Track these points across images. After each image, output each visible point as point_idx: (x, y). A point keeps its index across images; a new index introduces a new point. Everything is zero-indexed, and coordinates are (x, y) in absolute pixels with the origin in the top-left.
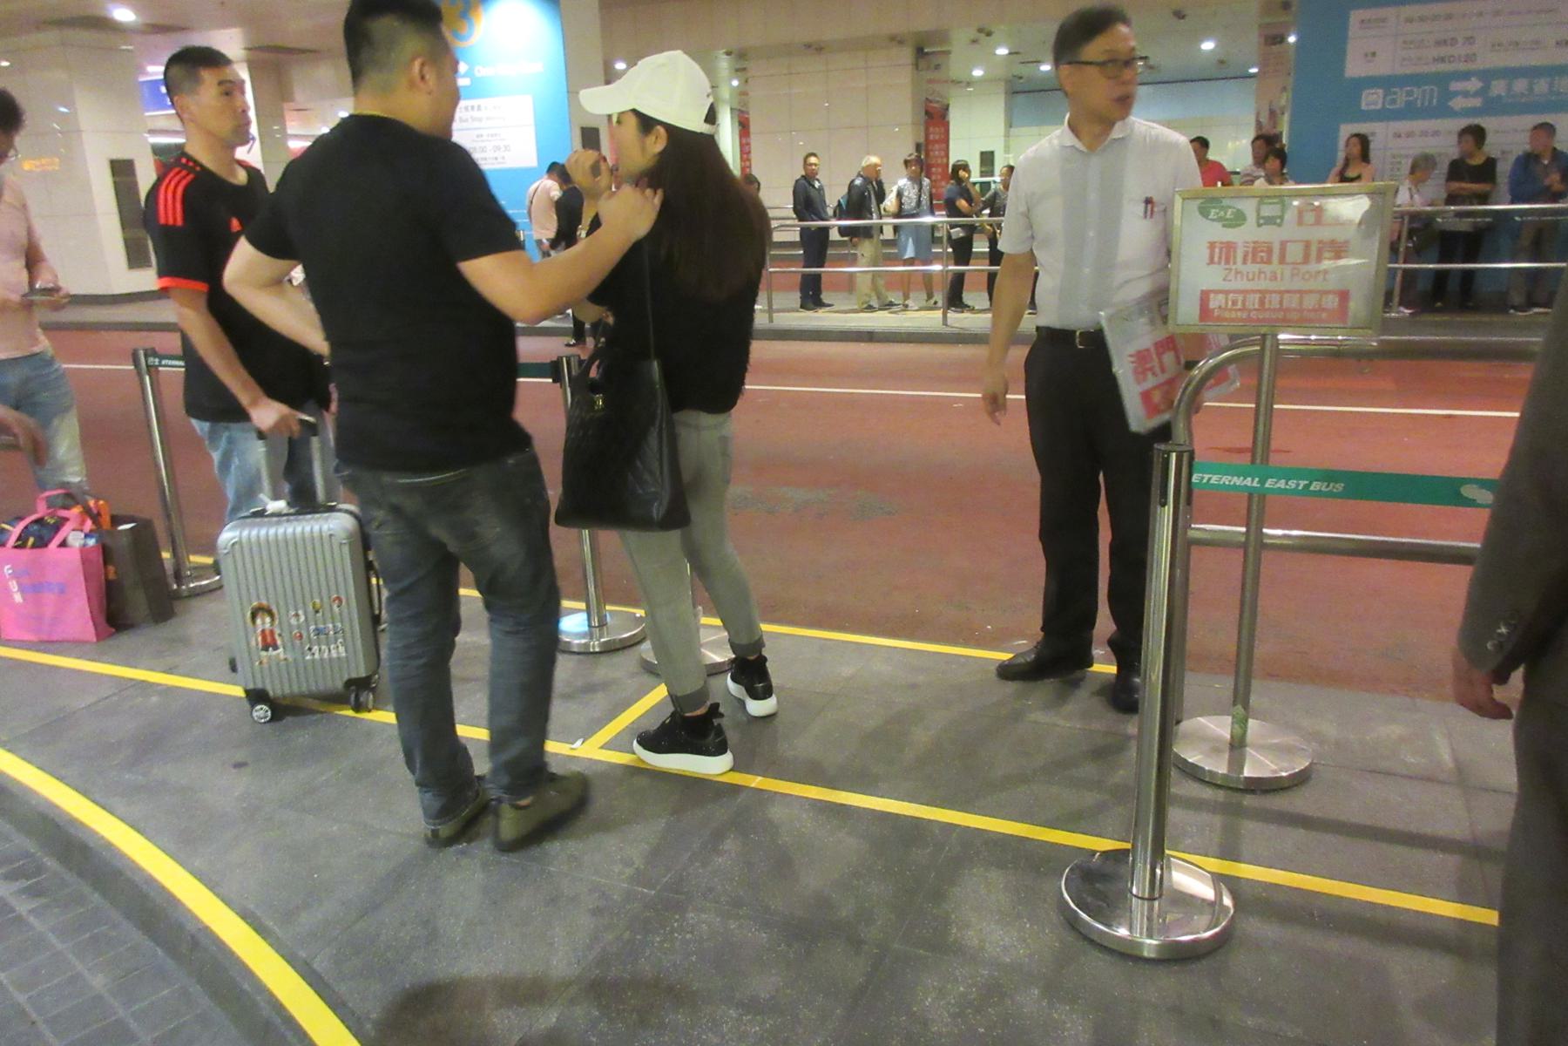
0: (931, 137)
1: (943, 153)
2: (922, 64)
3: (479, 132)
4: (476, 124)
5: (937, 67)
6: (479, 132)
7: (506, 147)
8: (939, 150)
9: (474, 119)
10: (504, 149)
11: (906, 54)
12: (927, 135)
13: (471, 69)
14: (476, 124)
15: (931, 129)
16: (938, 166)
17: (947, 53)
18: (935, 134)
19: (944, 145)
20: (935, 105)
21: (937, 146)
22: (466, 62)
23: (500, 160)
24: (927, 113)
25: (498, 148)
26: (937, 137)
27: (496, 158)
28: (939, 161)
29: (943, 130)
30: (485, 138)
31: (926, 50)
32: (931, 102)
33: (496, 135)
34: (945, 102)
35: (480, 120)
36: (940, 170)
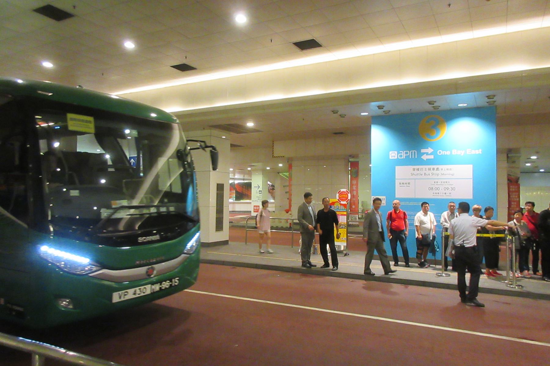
0: (511, 190)
4: (436, 177)
6: (436, 181)
8: (515, 195)
9: (433, 174)
10: (451, 189)
14: (436, 177)
15: (511, 187)
16: (514, 201)
17: (520, 157)
19: (517, 193)
21: (514, 194)
24: (508, 180)
26: (514, 190)
27: (445, 193)
28: (515, 199)
32: (510, 175)
33: (446, 182)
36: (515, 203)
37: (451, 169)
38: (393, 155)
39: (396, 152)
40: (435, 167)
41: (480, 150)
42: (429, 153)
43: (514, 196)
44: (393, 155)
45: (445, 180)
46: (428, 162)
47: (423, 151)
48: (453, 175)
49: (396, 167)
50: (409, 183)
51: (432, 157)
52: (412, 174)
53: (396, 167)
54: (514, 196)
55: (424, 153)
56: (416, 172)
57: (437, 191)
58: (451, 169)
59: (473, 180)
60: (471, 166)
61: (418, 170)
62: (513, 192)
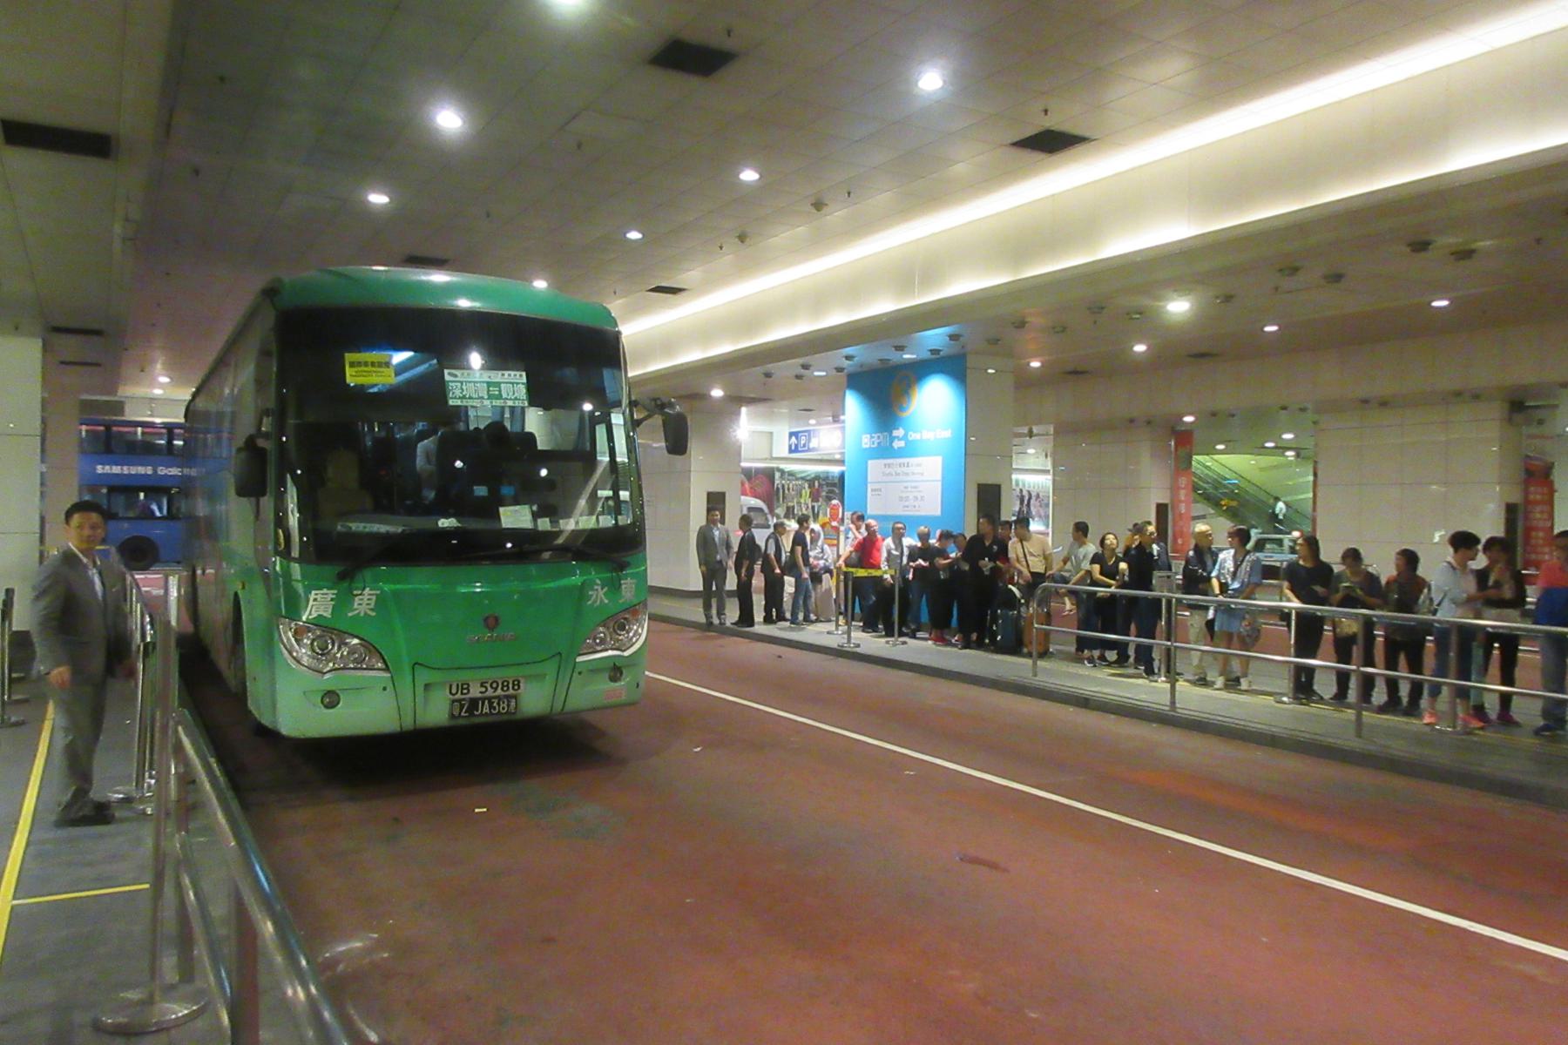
1: (1545, 516)
2: (1518, 418)
3: (906, 484)
4: (905, 478)
5: (1541, 422)
6: (906, 484)
7: (922, 497)
8: (1542, 512)
11: (1495, 411)
12: (1526, 492)
13: (906, 435)
14: (905, 478)
15: (1532, 489)
17: (1556, 406)
18: (1536, 494)
20: (1537, 463)
21: (1538, 508)
22: (904, 429)
23: (917, 508)
25: (916, 498)
29: (1545, 490)
30: (909, 489)
31: (1527, 404)
34: (1550, 459)
35: (907, 474)
37: (919, 465)
38: (866, 442)
39: (868, 436)
40: (905, 460)
41: (950, 431)
42: (901, 436)
43: (1538, 516)
44: (866, 440)
45: (913, 484)
46: (899, 454)
47: (895, 433)
48: (922, 474)
49: (870, 462)
50: (880, 490)
51: (902, 444)
52: (884, 473)
53: (870, 462)
54: (1538, 516)
55: (895, 437)
56: (888, 470)
57: (907, 503)
58: (919, 465)
59: (942, 485)
60: (939, 460)
61: (889, 465)
62: (1537, 503)
